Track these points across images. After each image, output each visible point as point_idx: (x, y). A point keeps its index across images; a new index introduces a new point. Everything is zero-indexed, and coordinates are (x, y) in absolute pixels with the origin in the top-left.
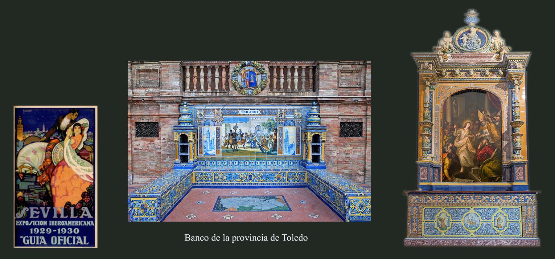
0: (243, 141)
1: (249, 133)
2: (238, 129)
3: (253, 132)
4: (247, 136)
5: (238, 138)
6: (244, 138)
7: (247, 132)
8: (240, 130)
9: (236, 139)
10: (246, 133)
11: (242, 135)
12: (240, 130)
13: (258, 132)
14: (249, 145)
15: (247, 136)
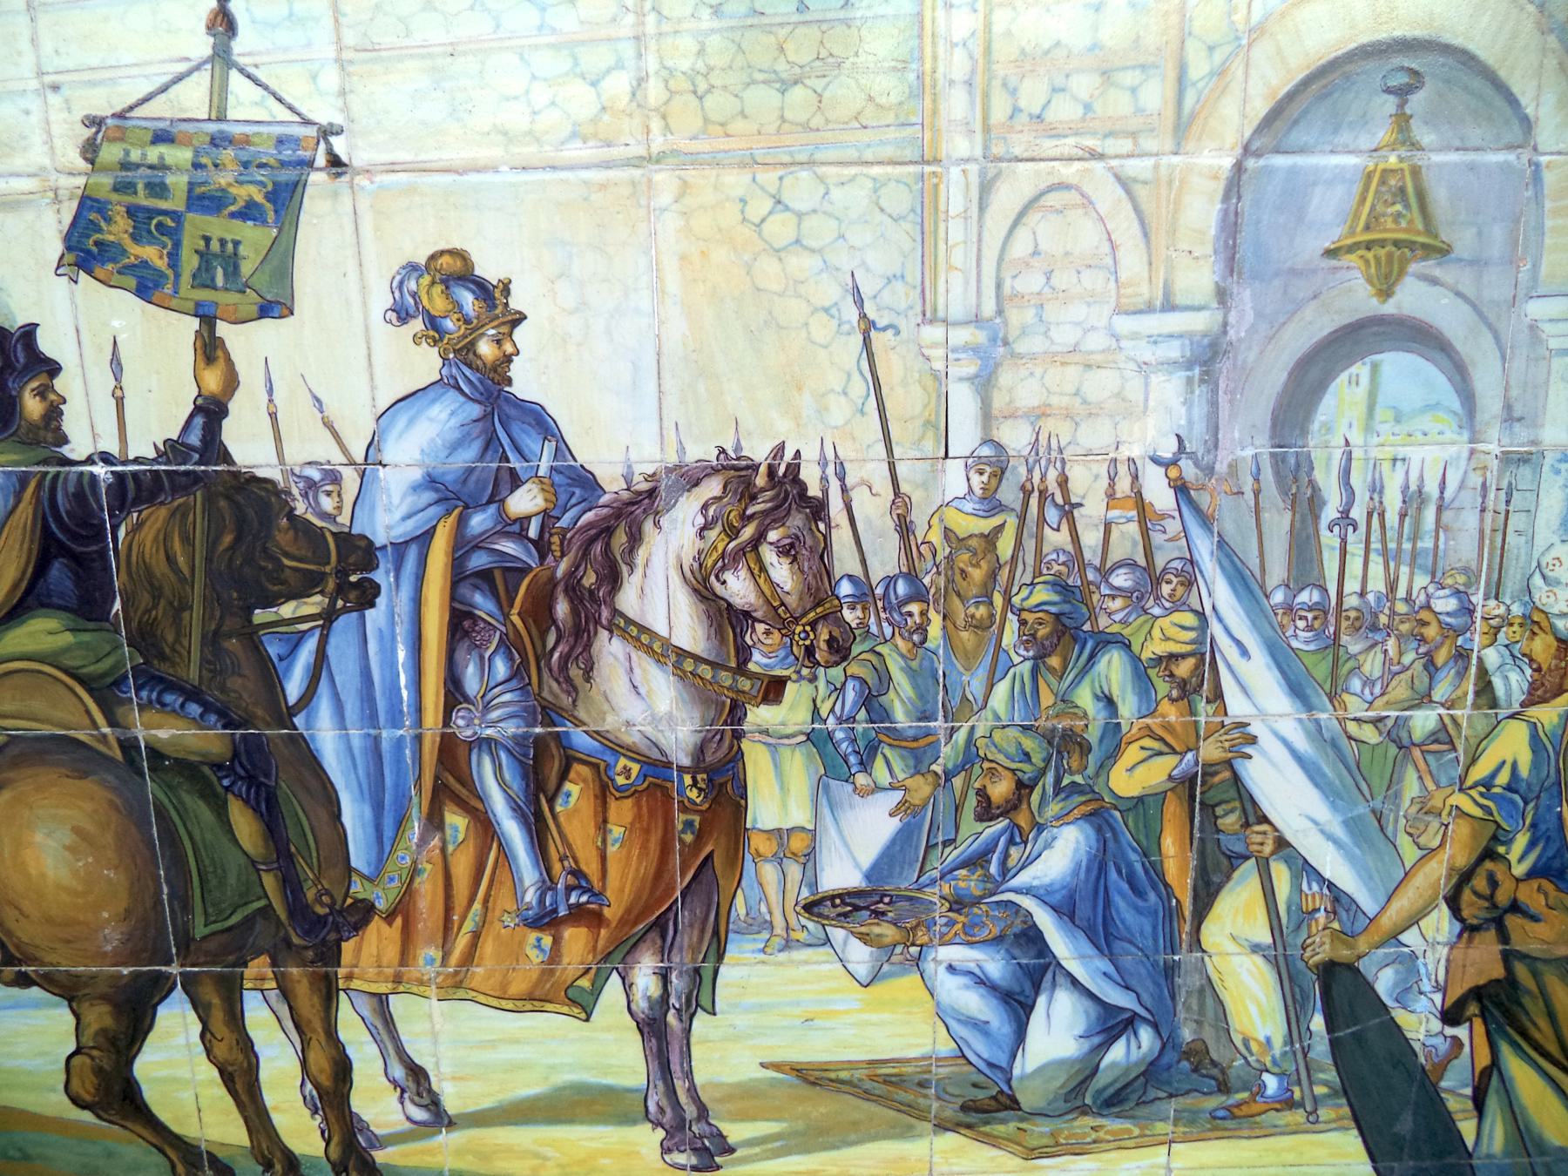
0: (613, 850)
1: (891, 485)
2: (344, 258)
3: (1118, 409)
4: (821, 627)
5: (362, 694)
6: (641, 704)
7: (806, 417)
8: (461, 310)
9: (266, 770)
10: (770, 499)
11: (541, 573)
12: (461, 310)
13: (1391, 433)
14: (902, 1017)
15: (821, 627)
